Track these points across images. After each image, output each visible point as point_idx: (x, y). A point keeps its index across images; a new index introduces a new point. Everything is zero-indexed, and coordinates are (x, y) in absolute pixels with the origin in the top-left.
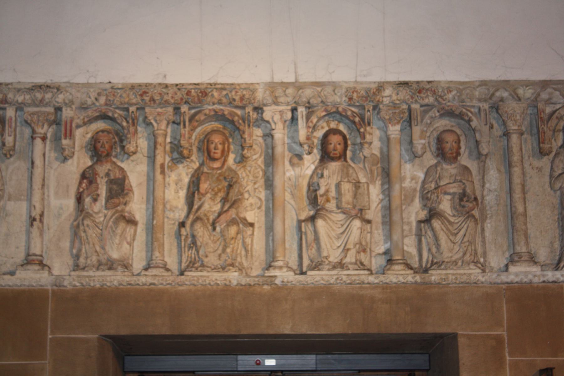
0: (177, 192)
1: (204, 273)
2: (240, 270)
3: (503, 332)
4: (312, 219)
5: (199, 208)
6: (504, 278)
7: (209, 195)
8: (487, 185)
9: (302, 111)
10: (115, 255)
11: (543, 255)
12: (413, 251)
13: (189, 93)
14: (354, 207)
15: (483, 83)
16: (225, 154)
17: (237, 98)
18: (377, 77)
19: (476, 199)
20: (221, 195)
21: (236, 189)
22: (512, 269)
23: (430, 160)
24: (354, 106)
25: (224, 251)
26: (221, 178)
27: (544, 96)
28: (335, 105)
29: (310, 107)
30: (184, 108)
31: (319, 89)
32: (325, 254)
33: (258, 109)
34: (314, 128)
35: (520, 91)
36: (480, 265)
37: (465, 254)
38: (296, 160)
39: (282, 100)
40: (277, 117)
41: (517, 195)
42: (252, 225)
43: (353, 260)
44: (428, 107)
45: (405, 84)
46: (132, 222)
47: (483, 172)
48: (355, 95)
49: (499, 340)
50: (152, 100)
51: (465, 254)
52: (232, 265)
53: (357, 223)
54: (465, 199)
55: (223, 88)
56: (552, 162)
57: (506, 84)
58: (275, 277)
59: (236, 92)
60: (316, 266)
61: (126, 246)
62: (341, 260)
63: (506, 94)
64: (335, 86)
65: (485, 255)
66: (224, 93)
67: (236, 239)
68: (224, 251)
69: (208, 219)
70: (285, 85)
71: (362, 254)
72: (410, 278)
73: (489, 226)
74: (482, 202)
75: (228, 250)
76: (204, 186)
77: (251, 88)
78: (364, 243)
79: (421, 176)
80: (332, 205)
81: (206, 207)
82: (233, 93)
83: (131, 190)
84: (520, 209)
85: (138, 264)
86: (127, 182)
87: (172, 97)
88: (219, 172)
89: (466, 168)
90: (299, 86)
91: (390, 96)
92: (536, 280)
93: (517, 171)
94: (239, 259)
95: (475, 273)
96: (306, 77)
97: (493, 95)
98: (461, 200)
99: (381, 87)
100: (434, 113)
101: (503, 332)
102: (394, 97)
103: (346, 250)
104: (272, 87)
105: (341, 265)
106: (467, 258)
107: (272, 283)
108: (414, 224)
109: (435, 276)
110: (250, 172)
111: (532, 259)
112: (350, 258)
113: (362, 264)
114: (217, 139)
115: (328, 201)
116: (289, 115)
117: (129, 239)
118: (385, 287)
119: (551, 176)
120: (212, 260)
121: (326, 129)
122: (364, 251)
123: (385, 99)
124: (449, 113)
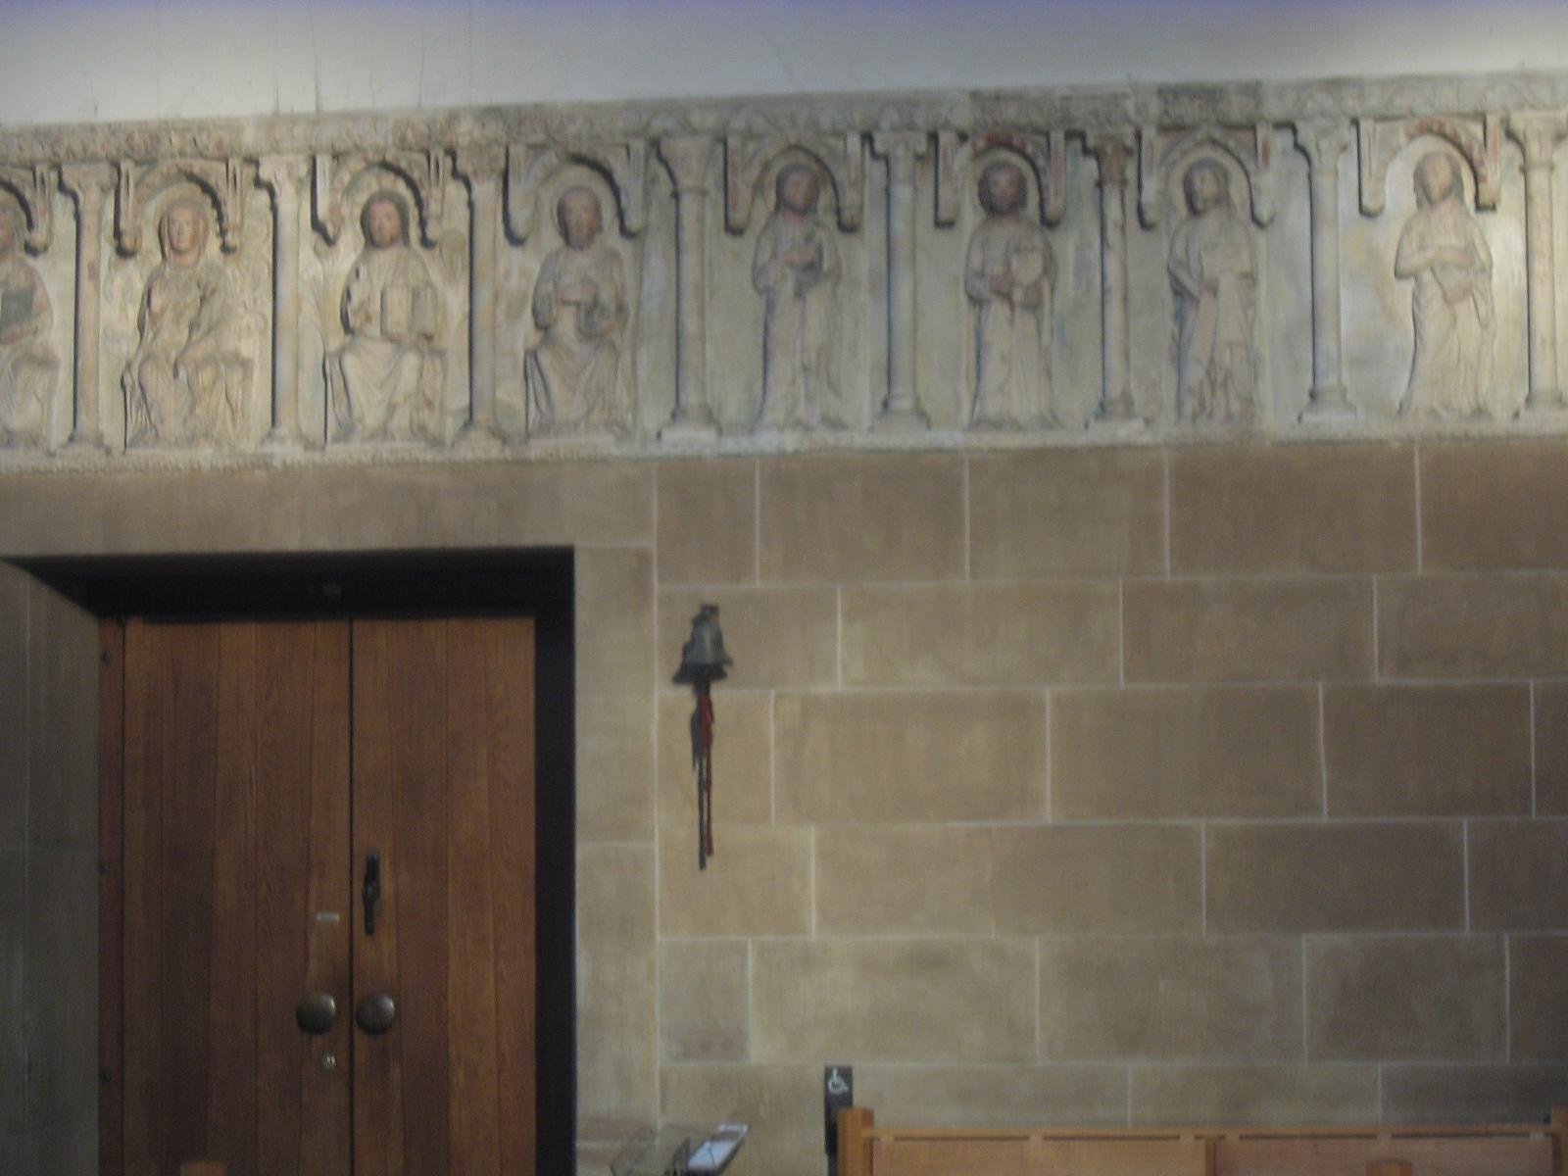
0: (123, 309)
1: (158, 451)
2: (218, 443)
3: (650, 543)
4: (340, 355)
5: (155, 337)
6: (655, 450)
7: (169, 315)
8: (647, 285)
9: (324, 163)
10: (17, 423)
11: (733, 408)
12: (520, 404)
13: (129, 139)
14: (410, 329)
15: (632, 106)
16: (198, 241)
17: (211, 146)
18: (454, 97)
19: (621, 308)
20: (190, 314)
21: (217, 302)
22: (669, 436)
23: (551, 239)
24: (410, 149)
25: (192, 411)
26: (193, 284)
27: (738, 124)
28: (377, 149)
29: (337, 156)
30: (126, 166)
31: (350, 124)
32: (357, 413)
33: (253, 161)
34: (349, 190)
35: (696, 119)
36: (616, 428)
37: (590, 410)
38: (322, 245)
39: (286, 144)
40: (282, 174)
41: (689, 303)
42: (245, 364)
43: (405, 423)
44: (538, 149)
45: (495, 112)
46: (46, 362)
47: (641, 261)
48: (410, 134)
49: (643, 558)
50: (70, 151)
51: (590, 410)
52: (207, 435)
53: (411, 360)
54: (596, 313)
55: (184, 128)
56: (758, 241)
57: (669, 107)
58: (272, 456)
59: (209, 135)
60: (346, 432)
61: (33, 407)
62: (386, 422)
63: (670, 124)
64: (375, 118)
65: (635, 407)
66: (189, 136)
67: (212, 391)
68: (192, 411)
69: (167, 358)
70: (293, 119)
71: (426, 411)
72: (494, 451)
73: (644, 358)
74: (637, 315)
75: (199, 410)
76: (157, 302)
77: (234, 126)
78: (428, 392)
79: (536, 267)
80: (374, 329)
81: (165, 335)
82: (204, 137)
83: (46, 306)
84: (691, 326)
85: (58, 433)
86: (39, 293)
87: (103, 147)
88: (190, 272)
89: (613, 256)
90: (317, 120)
91: (470, 133)
92: (708, 452)
93: (690, 259)
94: (219, 424)
95: (605, 443)
96: (334, 104)
97: (648, 124)
98: (589, 313)
99: (453, 118)
100: (551, 159)
101: (650, 543)
102: (477, 134)
103: (392, 408)
104: (272, 123)
105: (384, 432)
106: (595, 417)
107: (267, 466)
108: (521, 356)
109: (537, 449)
110: (248, 270)
111: (710, 417)
112: (401, 420)
113: (423, 429)
114: (184, 217)
115: (368, 318)
116: (303, 170)
117: (40, 393)
118: (455, 468)
119: (754, 267)
120: (172, 426)
121: (375, 187)
122: (429, 404)
123: (461, 140)
124: (578, 159)
